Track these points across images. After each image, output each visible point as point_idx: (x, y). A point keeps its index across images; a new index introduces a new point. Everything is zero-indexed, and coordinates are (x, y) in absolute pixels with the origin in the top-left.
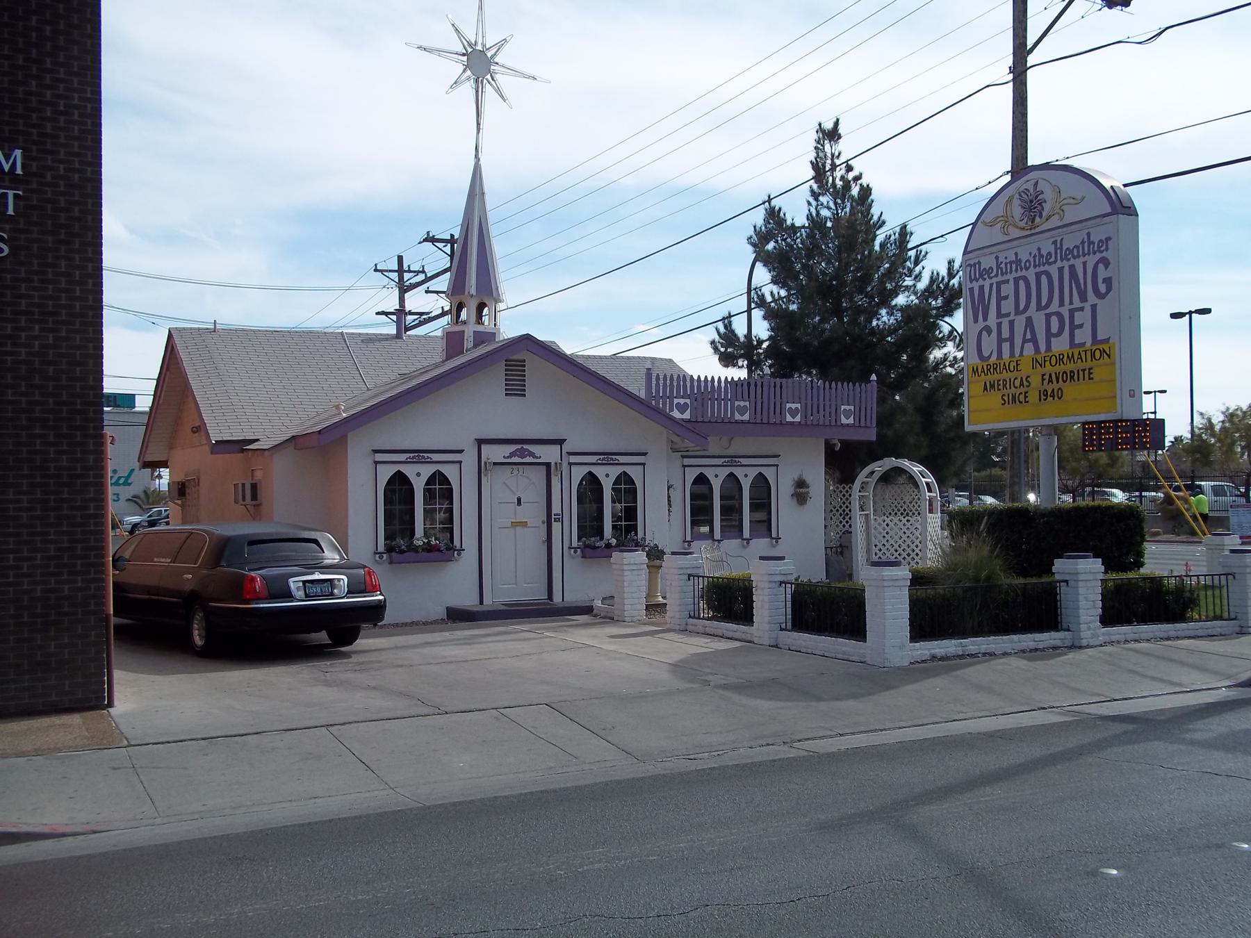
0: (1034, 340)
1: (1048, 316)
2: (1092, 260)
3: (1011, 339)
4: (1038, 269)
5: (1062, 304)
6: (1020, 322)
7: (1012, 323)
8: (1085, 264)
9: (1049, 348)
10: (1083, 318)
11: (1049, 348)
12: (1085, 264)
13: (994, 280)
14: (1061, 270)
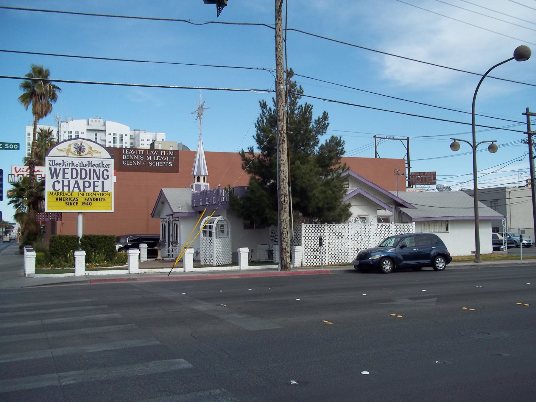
0: (79, 187)
1: (84, 182)
2: (102, 169)
3: (69, 186)
4: (81, 168)
5: (90, 178)
6: (72, 182)
7: (69, 182)
8: (99, 170)
9: (84, 190)
10: (99, 184)
11: (84, 190)
12: (99, 170)
13: (62, 167)
14: (90, 170)
